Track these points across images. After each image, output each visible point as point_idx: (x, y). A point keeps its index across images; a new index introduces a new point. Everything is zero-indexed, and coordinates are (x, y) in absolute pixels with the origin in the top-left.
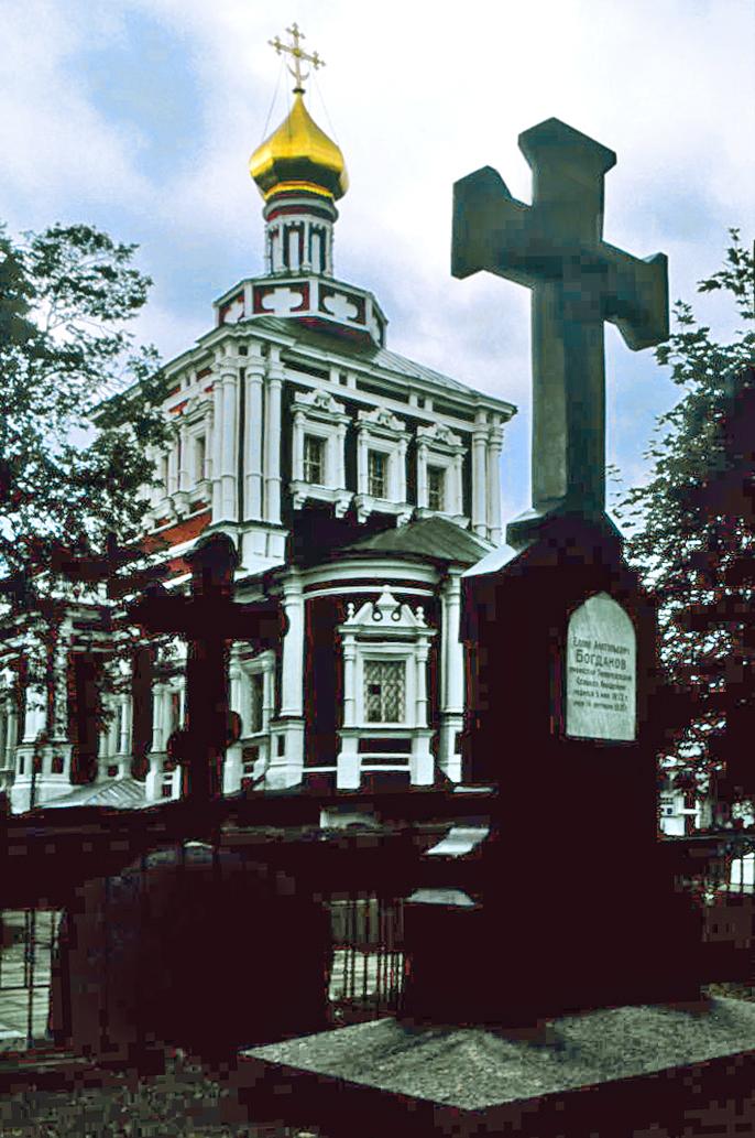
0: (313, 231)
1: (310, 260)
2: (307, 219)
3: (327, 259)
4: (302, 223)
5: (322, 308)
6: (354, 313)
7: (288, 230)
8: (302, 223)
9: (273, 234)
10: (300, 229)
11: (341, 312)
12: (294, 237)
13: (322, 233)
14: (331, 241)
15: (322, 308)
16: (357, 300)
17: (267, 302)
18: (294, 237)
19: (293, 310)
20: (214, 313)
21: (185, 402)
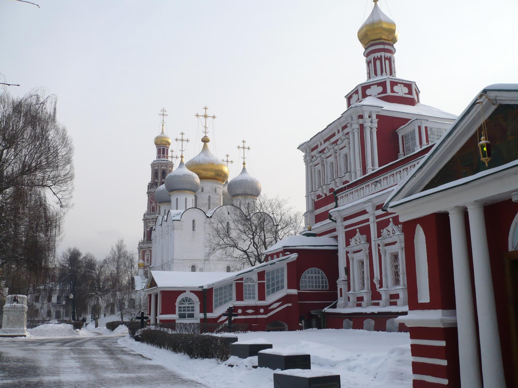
0: (386, 59)
1: (386, 72)
2: (383, 54)
3: (393, 70)
4: (381, 56)
5: (392, 91)
6: (406, 90)
7: (375, 59)
8: (381, 56)
9: (368, 63)
10: (380, 59)
11: (401, 91)
12: (378, 63)
13: (390, 59)
14: (394, 62)
15: (392, 91)
16: (409, 85)
17: (368, 92)
18: (378, 63)
19: (379, 94)
20: (345, 101)
21: (338, 140)
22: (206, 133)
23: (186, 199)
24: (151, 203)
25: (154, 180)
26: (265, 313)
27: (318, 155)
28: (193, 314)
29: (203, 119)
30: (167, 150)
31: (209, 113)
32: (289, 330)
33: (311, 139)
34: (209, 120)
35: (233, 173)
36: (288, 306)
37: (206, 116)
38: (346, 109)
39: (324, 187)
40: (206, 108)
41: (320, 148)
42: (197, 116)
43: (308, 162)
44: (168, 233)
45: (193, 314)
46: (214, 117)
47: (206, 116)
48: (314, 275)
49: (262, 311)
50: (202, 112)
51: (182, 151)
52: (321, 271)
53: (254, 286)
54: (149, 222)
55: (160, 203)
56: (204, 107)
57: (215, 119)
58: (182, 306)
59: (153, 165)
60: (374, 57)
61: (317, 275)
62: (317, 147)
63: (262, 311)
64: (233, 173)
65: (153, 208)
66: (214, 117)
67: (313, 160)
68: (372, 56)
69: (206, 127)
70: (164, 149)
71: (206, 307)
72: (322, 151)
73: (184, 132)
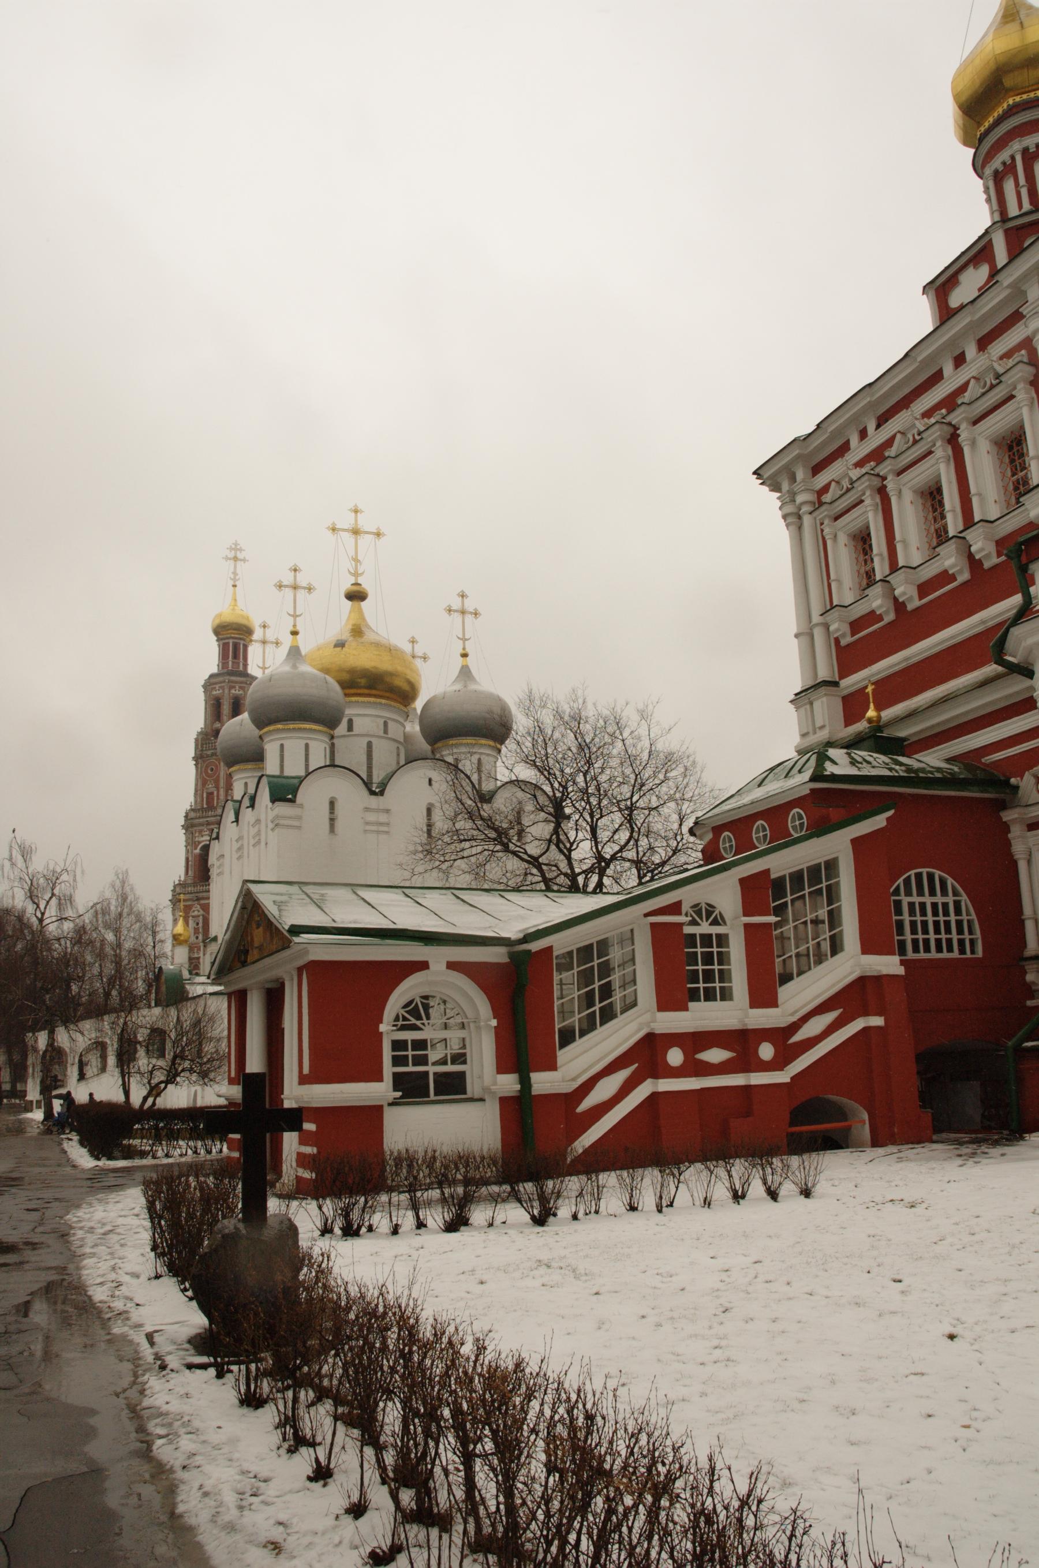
22: (356, 574)
23: (307, 746)
24: (204, 783)
25: (213, 723)
26: (779, 1063)
27: (855, 473)
28: (462, 1075)
29: (348, 538)
30: (246, 647)
31: (365, 523)
32: (876, 1142)
33: (818, 426)
34: (366, 541)
35: (434, 684)
36: (866, 1030)
37: (356, 532)
38: (931, 329)
39: (896, 579)
40: (356, 511)
41: (859, 450)
42: (334, 530)
43: (805, 509)
44: (259, 842)
45: (462, 1075)
46: (378, 535)
47: (356, 532)
48: (928, 900)
49: (766, 1051)
50: (346, 521)
51: (295, 616)
52: (950, 881)
53: (722, 940)
54: (200, 832)
55: (230, 765)
56: (351, 506)
57: (383, 539)
58: (409, 1036)
59: (209, 685)
60: (1025, 151)
61: (939, 899)
62: (845, 448)
63: (766, 1051)
64: (434, 684)
65: (210, 795)
66: (378, 535)
67: (827, 498)
68: (1016, 146)
69: (356, 560)
70: (236, 647)
71: (524, 1043)
72: (878, 455)
73: (300, 566)
